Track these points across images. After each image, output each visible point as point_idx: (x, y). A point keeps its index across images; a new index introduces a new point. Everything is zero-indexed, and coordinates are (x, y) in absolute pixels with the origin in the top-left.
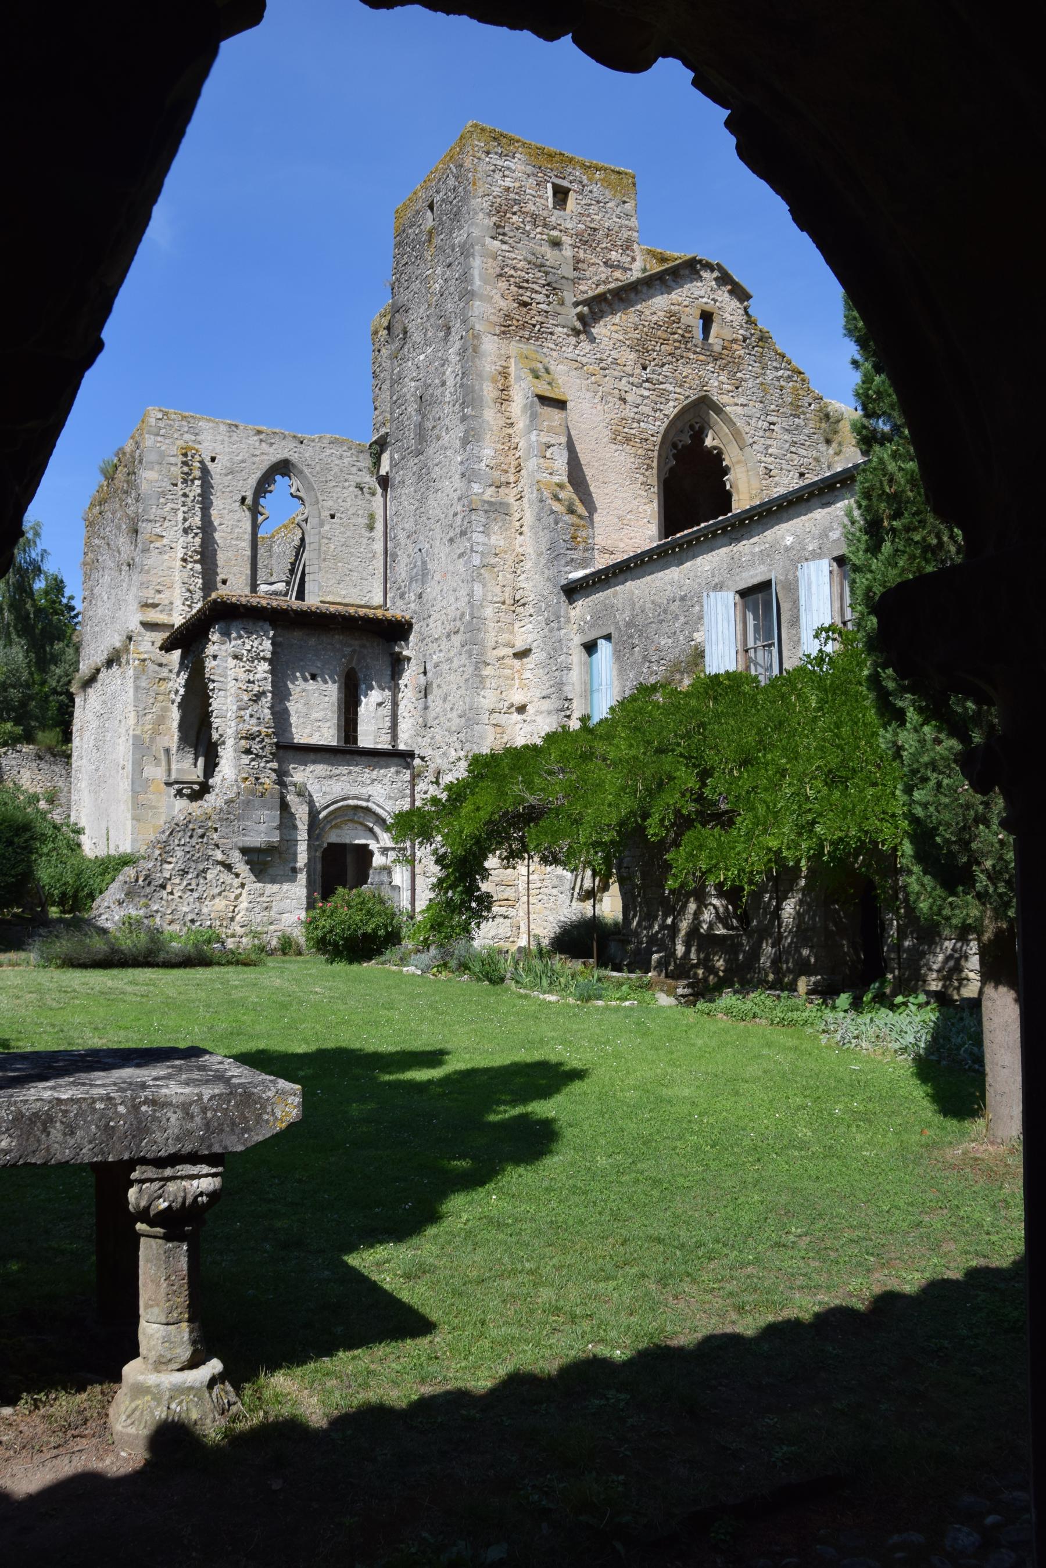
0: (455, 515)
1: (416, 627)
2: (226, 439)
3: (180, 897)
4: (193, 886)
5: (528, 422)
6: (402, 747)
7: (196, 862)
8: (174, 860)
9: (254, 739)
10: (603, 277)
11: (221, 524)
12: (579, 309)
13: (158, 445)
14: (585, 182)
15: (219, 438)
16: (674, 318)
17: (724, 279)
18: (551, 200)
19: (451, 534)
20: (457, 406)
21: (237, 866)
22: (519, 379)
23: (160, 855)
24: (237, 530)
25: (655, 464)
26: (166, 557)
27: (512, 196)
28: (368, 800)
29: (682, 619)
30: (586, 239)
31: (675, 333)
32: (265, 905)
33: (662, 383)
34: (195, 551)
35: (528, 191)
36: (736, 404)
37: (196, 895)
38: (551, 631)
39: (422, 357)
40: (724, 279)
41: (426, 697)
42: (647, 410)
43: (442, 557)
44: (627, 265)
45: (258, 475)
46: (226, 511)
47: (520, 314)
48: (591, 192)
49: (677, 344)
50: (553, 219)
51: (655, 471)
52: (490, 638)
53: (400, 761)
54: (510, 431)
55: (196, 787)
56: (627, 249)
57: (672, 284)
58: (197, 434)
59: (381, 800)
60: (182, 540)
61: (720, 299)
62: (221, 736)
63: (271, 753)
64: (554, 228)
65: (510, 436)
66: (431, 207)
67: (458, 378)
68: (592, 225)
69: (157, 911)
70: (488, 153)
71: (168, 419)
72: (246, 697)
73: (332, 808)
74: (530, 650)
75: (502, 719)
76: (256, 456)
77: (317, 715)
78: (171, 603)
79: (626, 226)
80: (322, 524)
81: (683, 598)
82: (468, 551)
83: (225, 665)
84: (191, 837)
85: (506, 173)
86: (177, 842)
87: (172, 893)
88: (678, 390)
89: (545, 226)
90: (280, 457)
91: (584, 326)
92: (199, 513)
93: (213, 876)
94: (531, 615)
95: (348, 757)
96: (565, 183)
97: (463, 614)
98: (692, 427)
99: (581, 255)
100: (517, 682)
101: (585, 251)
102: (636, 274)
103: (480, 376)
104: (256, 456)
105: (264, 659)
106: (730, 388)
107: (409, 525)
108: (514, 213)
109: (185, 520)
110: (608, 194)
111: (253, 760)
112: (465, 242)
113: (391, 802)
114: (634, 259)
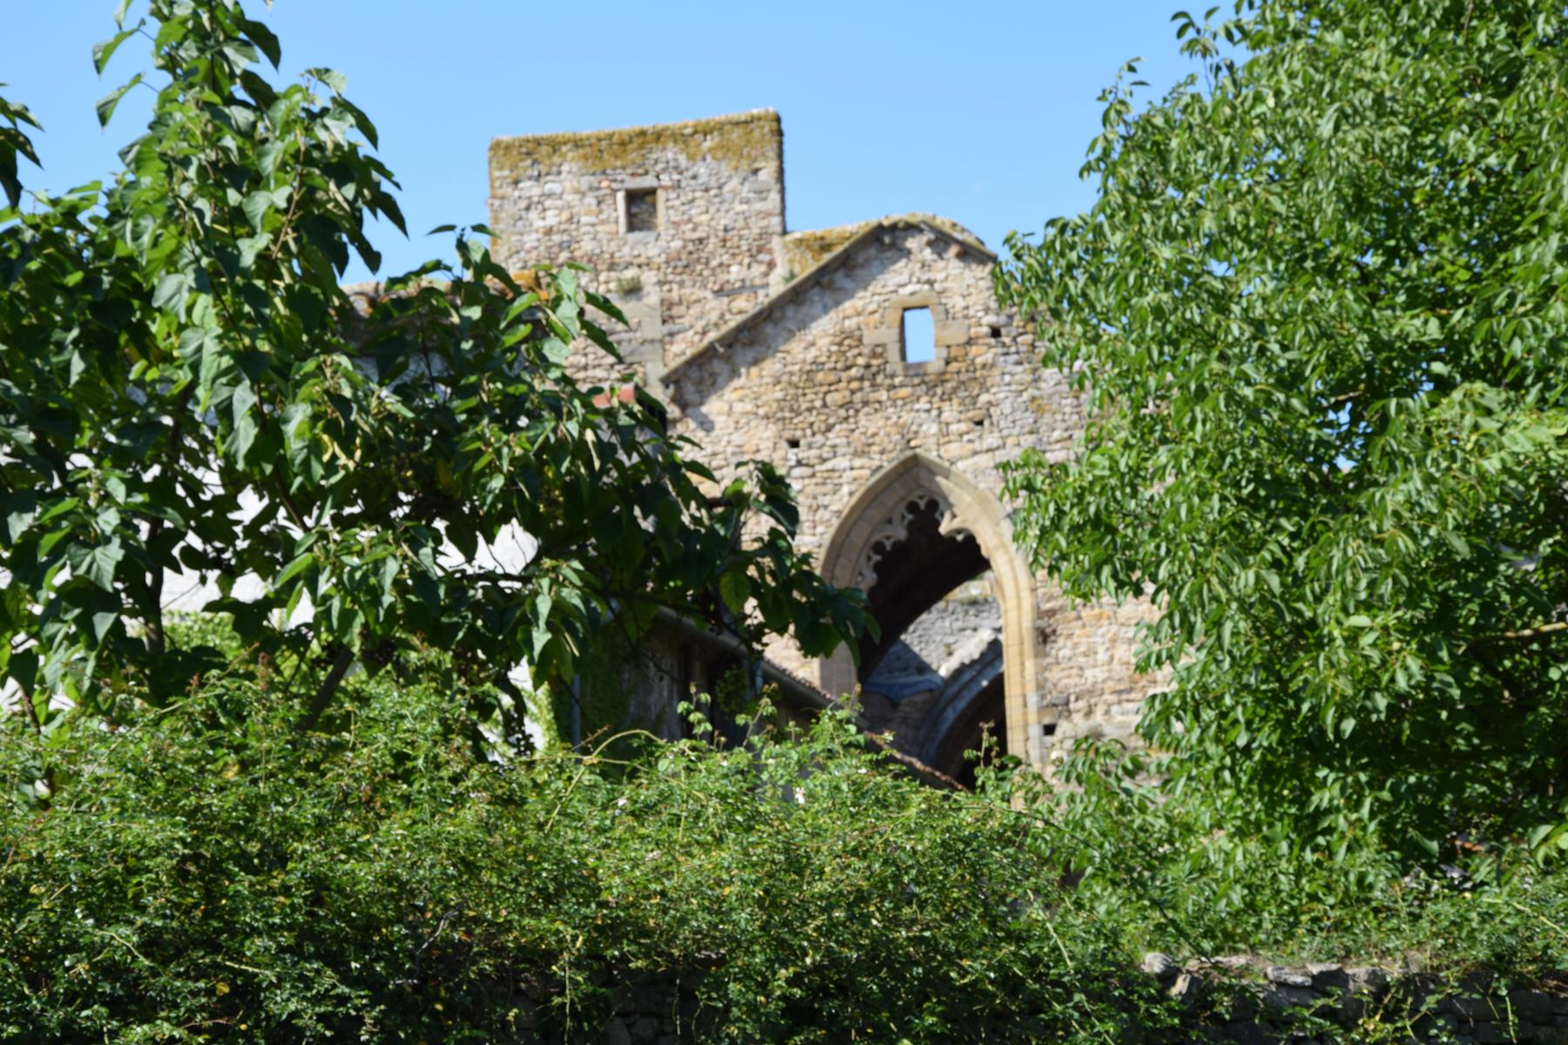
10: (714, 317)
16: (848, 339)
17: (941, 241)
18: (622, 220)
27: (556, 238)
30: (689, 261)
31: (849, 368)
35: (584, 219)
36: (975, 453)
40: (941, 241)
44: (758, 282)
48: (694, 177)
49: (855, 385)
50: (626, 250)
56: (759, 251)
57: (848, 284)
61: (940, 276)
64: (628, 265)
68: (696, 235)
70: (516, 182)
79: (758, 213)
88: (857, 462)
89: (612, 267)
96: (648, 182)
98: (913, 507)
99: (675, 296)
101: (681, 284)
102: (777, 286)
106: (963, 427)
110: (725, 169)
114: (771, 265)
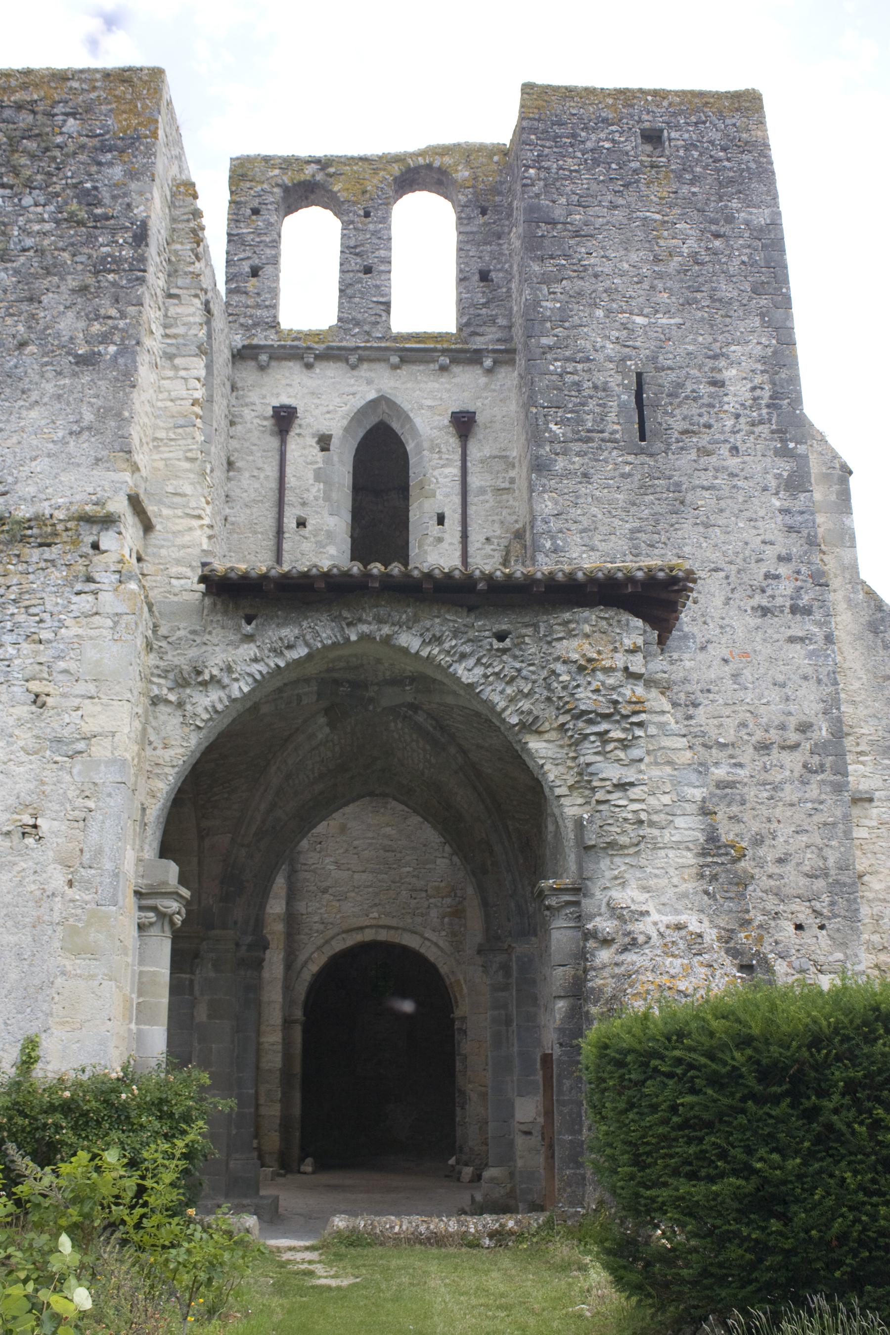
5: (833, 497)
39: (639, 320)
67: (766, 394)
94: (861, 753)
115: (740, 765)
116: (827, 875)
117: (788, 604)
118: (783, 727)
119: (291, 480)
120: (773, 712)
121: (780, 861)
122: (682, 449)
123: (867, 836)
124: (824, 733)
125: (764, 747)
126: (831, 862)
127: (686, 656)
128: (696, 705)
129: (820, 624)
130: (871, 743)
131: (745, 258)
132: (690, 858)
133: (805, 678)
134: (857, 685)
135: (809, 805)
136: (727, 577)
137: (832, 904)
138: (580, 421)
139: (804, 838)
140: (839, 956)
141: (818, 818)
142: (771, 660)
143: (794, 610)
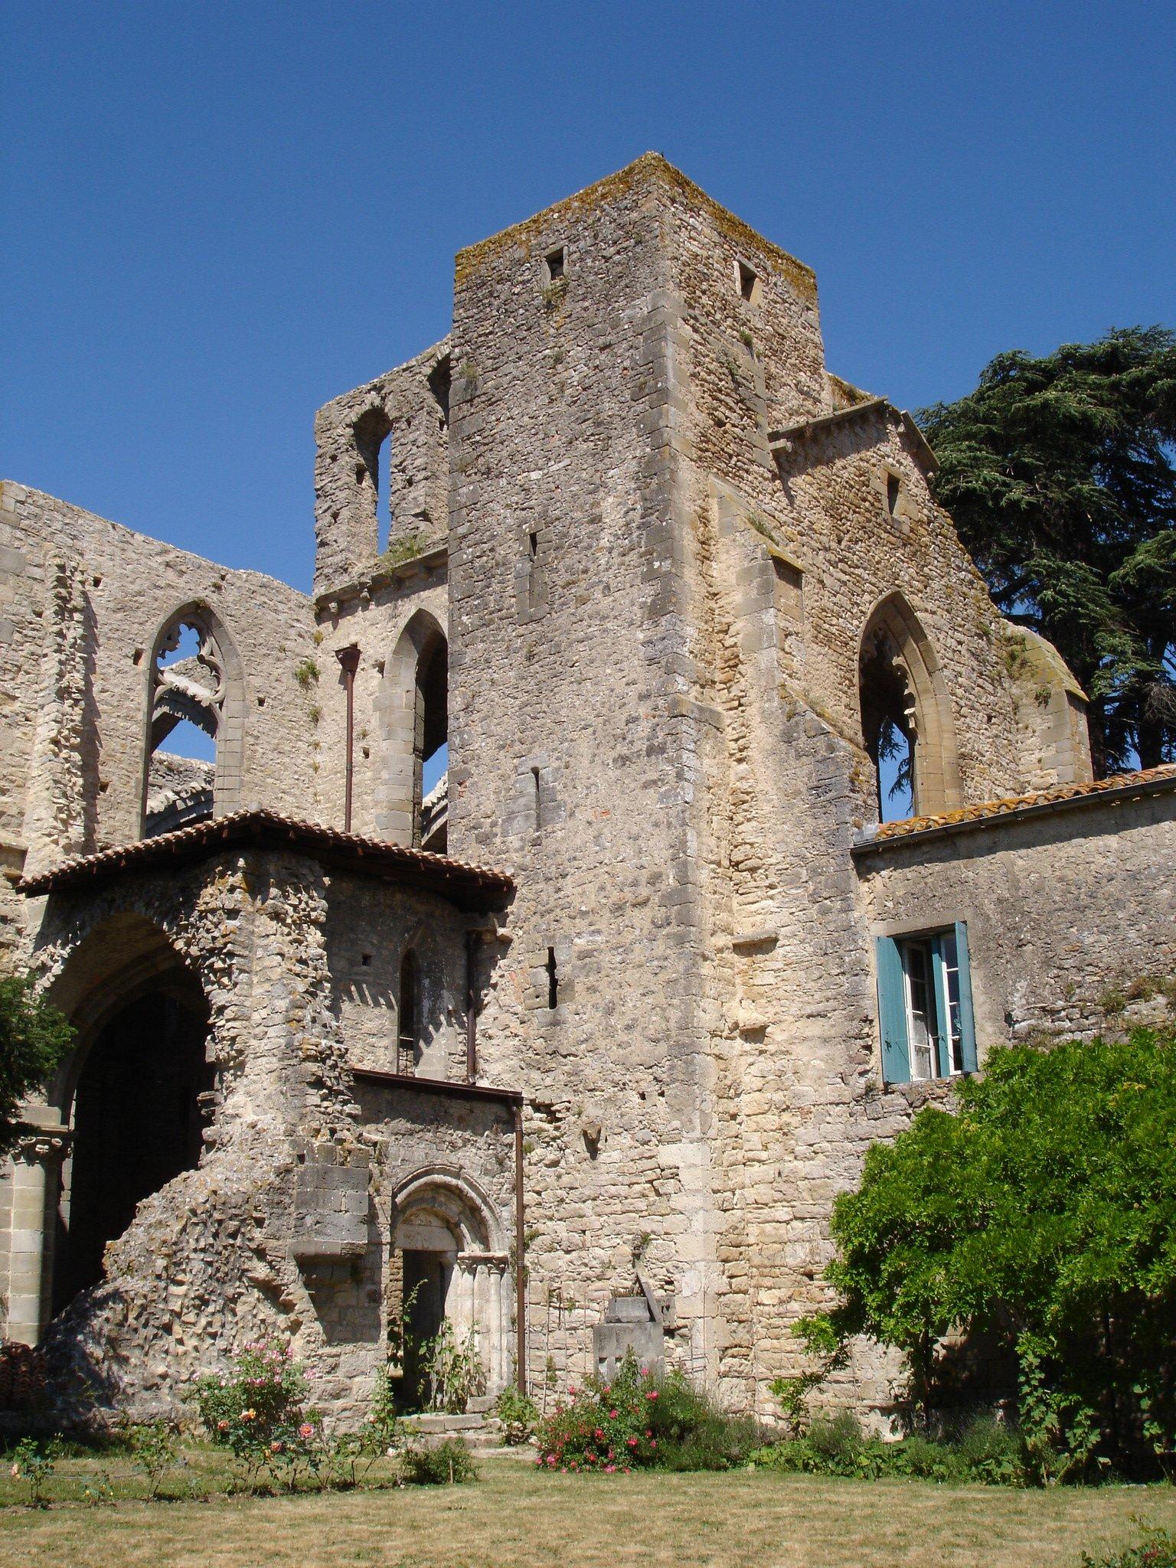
0: (632, 720)
1: (522, 892)
2: (118, 552)
3: (196, 1349)
4: (216, 1328)
5: (754, 594)
6: (483, 1083)
7: (222, 1282)
8: (188, 1278)
9: (323, 1061)
11: (103, 691)
12: (781, 443)
13: (17, 543)
14: (770, 269)
15: (108, 549)
19: (622, 749)
20: (633, 556)
21: (292, 1288)
22: (727, 529)
23: (166, 1268)
24: (128, 704)
25: (856, 680)
26: (17, 733)
28: (457, 1176)
29: (1132, 908)
31: (865, 500)
32: (330, 1361)
33: (857, 567)
34: (73, 730)
36: (926, 610)
37: (221, 1344)
38: (824, 912)
39: (534, 475)
41: (553, 1003)
42: (845, 601)
43: (592, 782)
45: (161, 619)
46: (112, 670)
47: (714, 433)
51: (856, 690)
52: (706, 914)
53: (497, 1109)
54: (712, 604)
55: (57, 1141)
58: (75, 538)
59: (474, 1174)
60: (54, 706)
62: (240, 1052)
63: (349, 1088)
64: (744, 324)
65: (712, 610)
66: (555, 261)
67: (636, 516)
69: (164, 1377)
71: (34, 503)
72: (301, 986)
73: (411, 1187)
74: (776, 940)
75: (723, 1046)
76: (159, 587)
77: (370, 1025)
78: (21, 814)
80: (246, 713)
81: (1134, 876)
82: (672, 778)
83: (251, 928)
84: (216, 1235)
85: (693, 234)
86: (193, 1244)
87: (180, 1342)
90: (190, 597)
91: (786, 466)
92: (81, 667)
93: (246, 1308)
94: (771, 887)
95: (434, 1098)
96: (751, 266)
97: (655, 879)
100: (740, 991)
102: (825, 412)
103: (679, 515)
104: (159, 587)
105: (315, 923)
107: (506, 728)
108: (704, 292)
109: (61, 675)
110: (794, 293)
111: (324, 1098)
112: (648, 318)
113: (486, 1179)
115: (599, 932)
116: (668, 1037)
117: (644, 747)
118: (635, 884)
119: (357, 715)
120: (626, 872)
121: (628, 1027)
122: (563, 604)
123: (772, 981)
124: (671, 881)
125: (618, 909)
126: (672, 1024)
127: (558, 826)
128: (564, 876)
129: (670, 761)
130: (780, 872)
131: (627, 363)
132: (275, 1063)
133: (656, 825)
134: (767, 808)
135: (655, 963)
136: (594, 733)
137: (672, 1068)
138: (486, 605)
139: (650, 1000)
140: (676, 1124)
141: (664, 976)
142: (628, 812)
143: (650, 751)
